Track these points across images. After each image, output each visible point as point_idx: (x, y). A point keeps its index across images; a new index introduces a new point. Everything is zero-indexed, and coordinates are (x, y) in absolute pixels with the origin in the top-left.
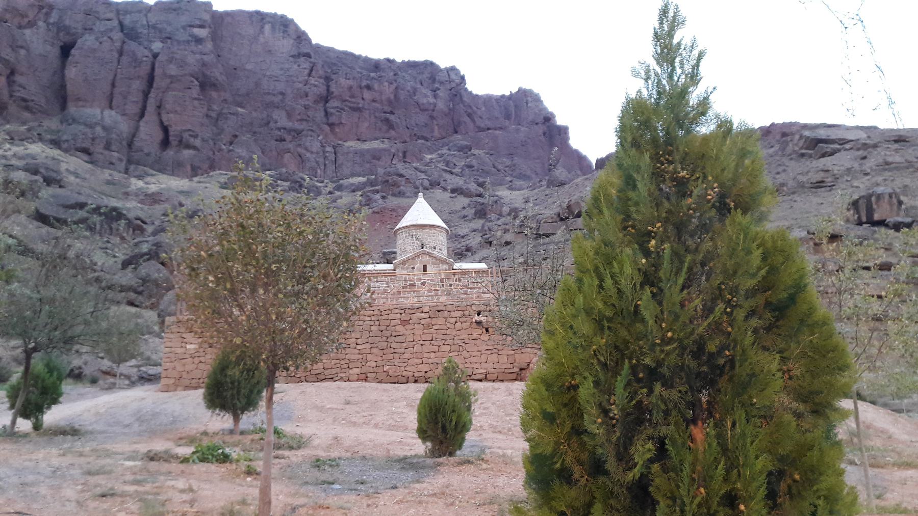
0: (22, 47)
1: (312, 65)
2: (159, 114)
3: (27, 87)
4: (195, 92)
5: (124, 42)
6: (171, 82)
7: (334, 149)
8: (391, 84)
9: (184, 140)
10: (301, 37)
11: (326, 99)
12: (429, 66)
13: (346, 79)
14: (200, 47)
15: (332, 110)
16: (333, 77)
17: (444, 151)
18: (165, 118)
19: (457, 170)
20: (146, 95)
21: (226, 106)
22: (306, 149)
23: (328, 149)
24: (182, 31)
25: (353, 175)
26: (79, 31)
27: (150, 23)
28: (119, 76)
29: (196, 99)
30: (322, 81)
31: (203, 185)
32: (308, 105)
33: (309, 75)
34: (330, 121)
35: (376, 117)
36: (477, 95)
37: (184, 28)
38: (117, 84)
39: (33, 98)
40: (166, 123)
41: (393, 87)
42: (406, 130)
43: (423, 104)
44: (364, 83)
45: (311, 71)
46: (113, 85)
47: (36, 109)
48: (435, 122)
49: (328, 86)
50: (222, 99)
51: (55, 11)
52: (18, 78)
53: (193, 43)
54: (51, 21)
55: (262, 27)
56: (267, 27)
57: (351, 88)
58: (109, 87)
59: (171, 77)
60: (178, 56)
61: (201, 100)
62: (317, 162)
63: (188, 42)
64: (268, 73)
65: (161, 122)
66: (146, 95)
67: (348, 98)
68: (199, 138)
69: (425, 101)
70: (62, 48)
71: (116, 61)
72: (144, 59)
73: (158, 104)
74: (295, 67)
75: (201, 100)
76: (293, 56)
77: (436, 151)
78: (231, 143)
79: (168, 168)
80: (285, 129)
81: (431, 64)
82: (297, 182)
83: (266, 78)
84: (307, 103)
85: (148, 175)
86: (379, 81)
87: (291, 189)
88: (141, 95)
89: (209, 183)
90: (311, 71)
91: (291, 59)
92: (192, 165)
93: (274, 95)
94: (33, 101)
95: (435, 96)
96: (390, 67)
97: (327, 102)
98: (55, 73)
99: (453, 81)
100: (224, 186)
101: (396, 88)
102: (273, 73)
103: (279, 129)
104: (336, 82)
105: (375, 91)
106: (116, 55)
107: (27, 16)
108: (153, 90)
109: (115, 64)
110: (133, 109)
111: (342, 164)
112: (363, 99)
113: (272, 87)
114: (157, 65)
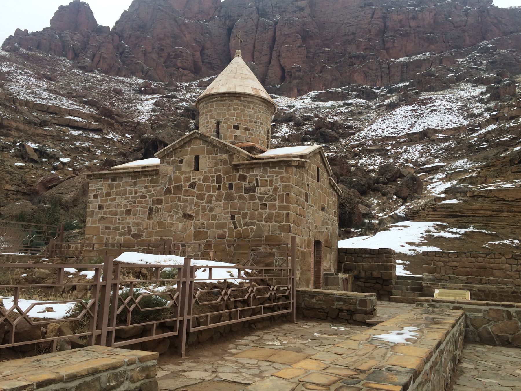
0: (207, 33)
1: (373, 10)
2: (279, 60)
3: (210, 56)
4: (299, 42)
5: (259, 20)
6: (285, 39)
7: (389, 65)
8: (431, 12)
11: (383, 31)
13: (397, 15)
14: (302, 13)
16: (388, 15)
19: (483, 67)
20: (271, 49)
22: (369, 68)
23: (384, 66)
24: (292, 5)
25: (402, 81)
26: (236, 18)
27: (273, 5)
28: (256, 41)
29: (299, 47)
30: (381, 20)
31: (302, 101)
33: (372, 18)
34: (386, 47)
35: (419, 38)
36: (502, 9)
37: (292, 3)
38: (256, 46)
39: (214, 62)
40: (283, 66)
41: (432, 14)
42: (443, 43)
43: (456, 22)
44: (410, 16)
45: (373, 14)
46: (254, 47)
47: (215, 68)
48: (466, 34)
49: (385, 23)
50: (316, 44)
51: (223, 9)
52: (206, 51)
53: (298, 12)
54: (221, 15)
57: (401, 21)
58: (252, 48)
59: (285, 35)
60: (288, 22)
61: (302, 47)
62: (376, 76)
63: (295, 11)
64: (345, 22)
65: (281, 65)
66: (271, 49)
67: (399, 28)
68: (302, 72)
69: (458, 20)
70: (228, 30)
71: (255, 31)
72: (270, 27)
73: (278, 55)
74: (362, 14)
75: (302, 47)
76: (361, 7)
77: (467, 55)
78: (321, 72)
79: (284, 93)
80: (354, 57)
83: (344, 26)
84: (370, 37)
86: (422, 12)
87: (357, 96)
88: (269, 49)
90: (373, 14)
91: (360, 9)
93: (348, 36)
94: (214, 63)
97: (384, 33)
98: (225, 46)
100: (314, 99)
101: (435, 15)
102: (348, 21)
103: (351, 58)
104: (390, 19)
105: (419, 20)
106: (254, 27)
107: (209, 15)
108: (275, 46)
109: (255, 34)
110: (265, 59)
111: (394, 75)
112: (410, 27)
113: (347, 31)
114: (277, 30)
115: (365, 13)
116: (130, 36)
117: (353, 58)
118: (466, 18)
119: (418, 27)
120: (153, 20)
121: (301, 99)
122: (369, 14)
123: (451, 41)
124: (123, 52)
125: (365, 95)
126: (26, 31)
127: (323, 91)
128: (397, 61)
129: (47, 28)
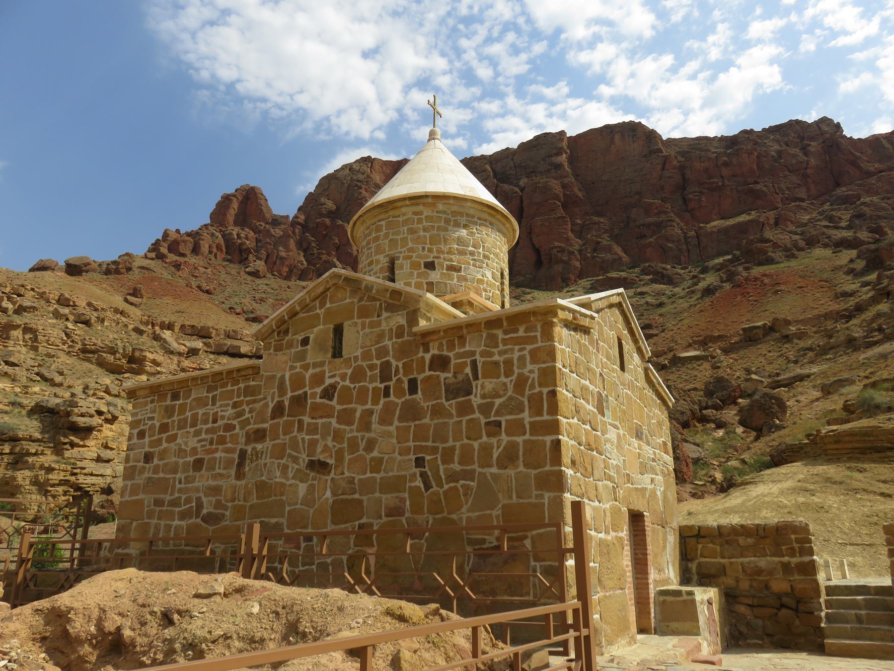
2: (531, 239)
7: (697, 233)
9: (553, 257)
10: (651, 135)
11: (682, 187)
12: (795, 126)
14: (559, 172)
15: (690, 196)
17: (827, 207)
18: (535, 240)
21: (588, 218)
24: (543, 163)
25: (719, 255)
32: (665, 197)
33: (663, 169)
35: (738, 191)
43: (792, 165)
45: (664, 164)
48: (809, 180)
49: (683, 175)
55: (613, 139)
56: (617, 137)
63: (549, 170)
65: (534, 246)
68: (566, 252)
72: (515, 195)
76: (645, 156)
80: (644, 225)
81: (797, 122)
82: (660, 272)
85: (525, 294)
89: (576, 291)
90: (664, 164)
92: (562, 278)
95: (806, 154)
96: (749, 138)
97: (683, 188)
99: (826, 132)
101: (757, 157)
103: (639, 227)
112: (722, 177)
115: (651, 163)
116: (317, 226)
117: (642, 227)
118: (806, 158)
119: (734, 176)
120: (349, 201)
121: (568, 292)
122: (658, 164)
123: (787, 192)
124: (308, 248)
125: (665, 279)
126: (178, 231)
127: (601, 277)
128: (708, 226)
129: (205, 225)
